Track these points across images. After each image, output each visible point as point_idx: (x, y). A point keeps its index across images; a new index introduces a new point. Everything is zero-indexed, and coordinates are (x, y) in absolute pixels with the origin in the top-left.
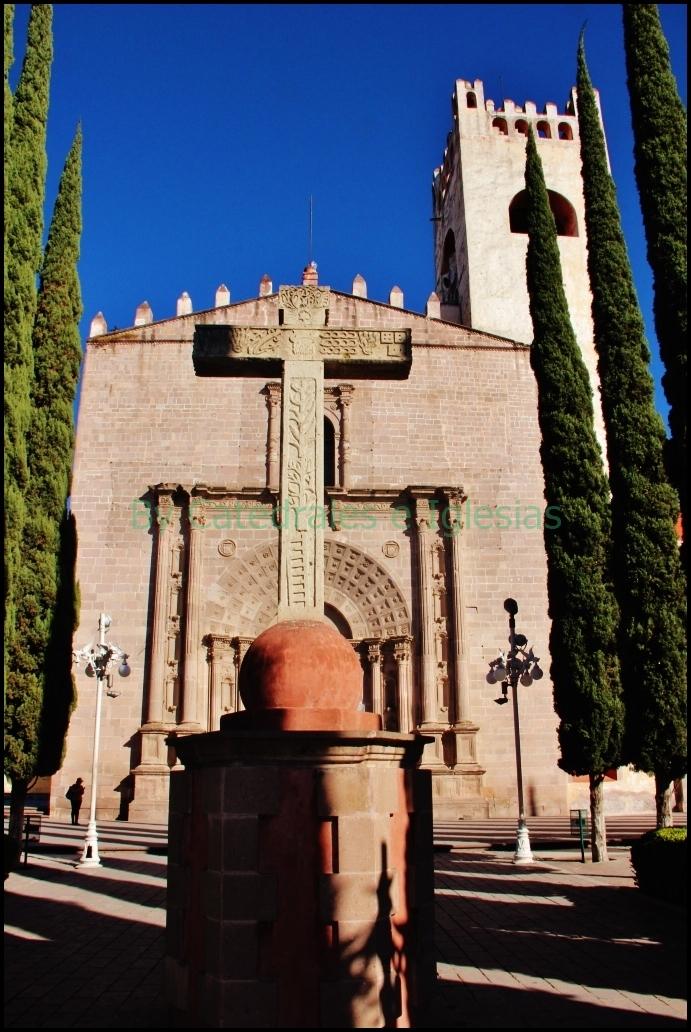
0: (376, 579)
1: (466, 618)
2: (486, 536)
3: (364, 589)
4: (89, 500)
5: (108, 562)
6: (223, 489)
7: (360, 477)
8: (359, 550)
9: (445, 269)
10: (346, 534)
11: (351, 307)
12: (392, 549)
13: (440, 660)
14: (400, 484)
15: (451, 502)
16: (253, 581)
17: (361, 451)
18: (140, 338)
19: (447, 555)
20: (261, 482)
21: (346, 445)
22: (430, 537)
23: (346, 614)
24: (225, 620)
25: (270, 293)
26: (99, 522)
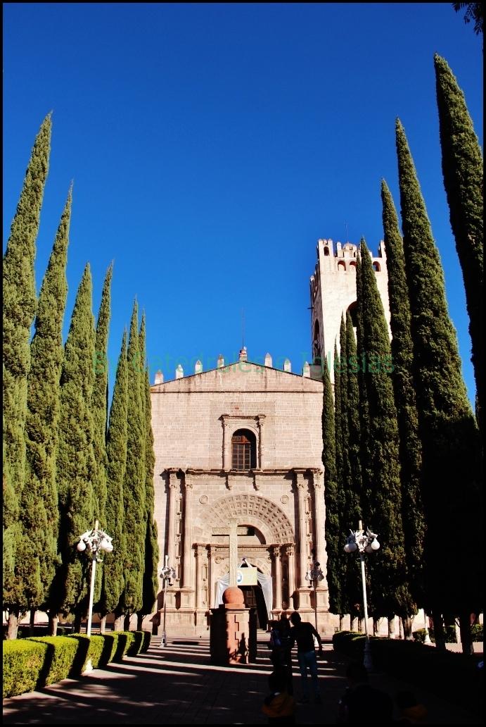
0: (277, 514)
6: (202, 470)
9: (316, 338)
10: (262, 492)
11: (264, 372)
12: (285, 499)
13: (309, 555)
14: (289, 466)
15: (314, 475)
17: (270, 449)
18: (157, 391)
20: (220, 466)
21: (262, 446)
22: (304, 493)
24: (203, 536)
25: (223, 366)
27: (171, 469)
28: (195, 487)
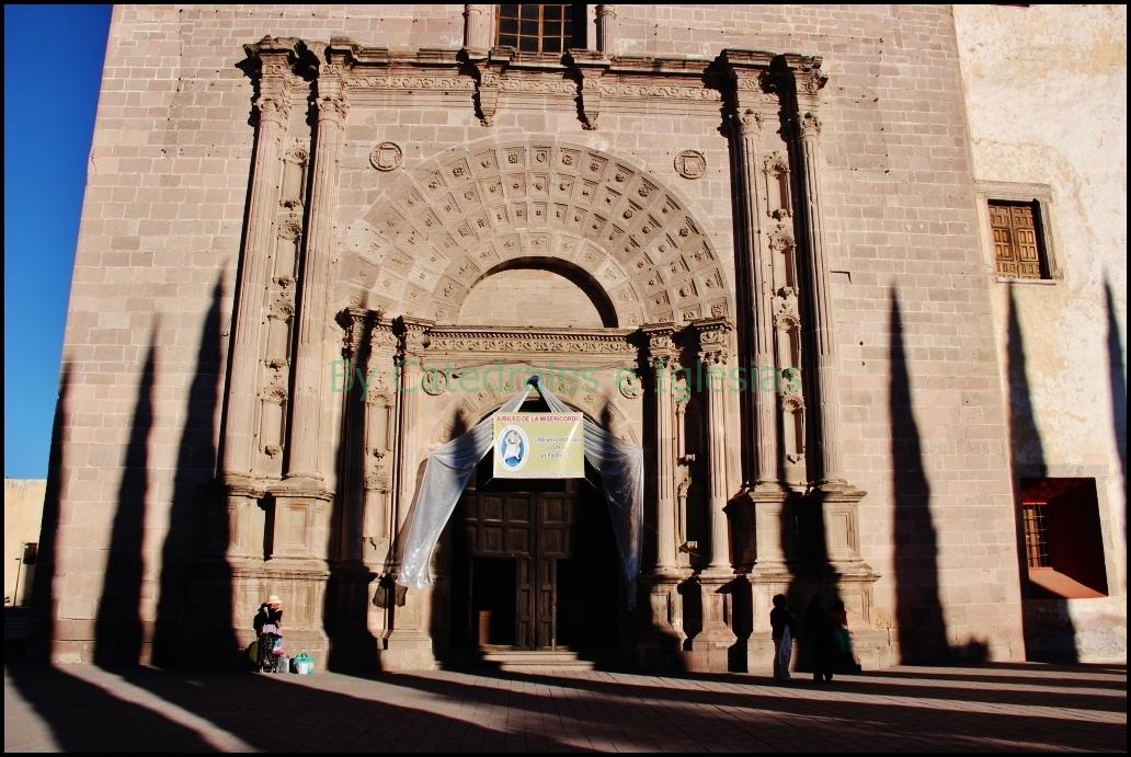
1: (833, 293)
2: (861, 150)
3: (640, 238)
4: (138, 73)
5: (165, 180)
6: (382, 52)
7: (633, 42)
8: (631, 162)
10: (606, 136)
12: (692, 164)
14: (709, 53)
16: (432, 219)
19: (796, 175)
22: (765, 142)
23: (607, 285)
26: (152, 111)
27: (267, 39)
28: (357, 115)
